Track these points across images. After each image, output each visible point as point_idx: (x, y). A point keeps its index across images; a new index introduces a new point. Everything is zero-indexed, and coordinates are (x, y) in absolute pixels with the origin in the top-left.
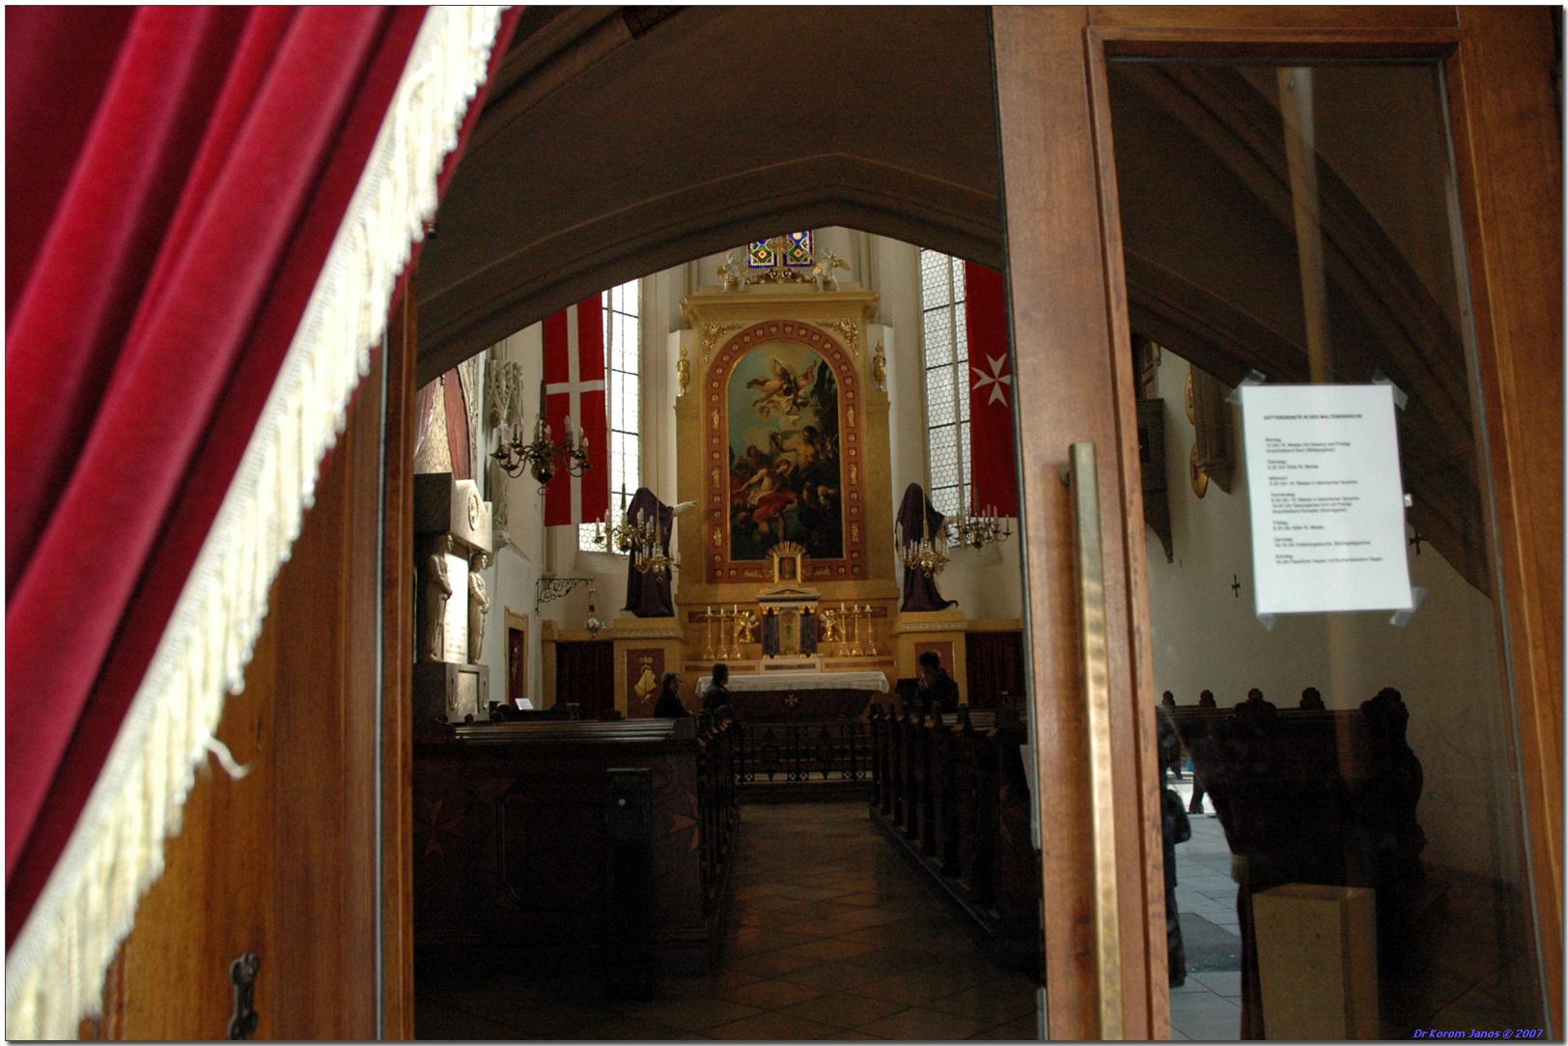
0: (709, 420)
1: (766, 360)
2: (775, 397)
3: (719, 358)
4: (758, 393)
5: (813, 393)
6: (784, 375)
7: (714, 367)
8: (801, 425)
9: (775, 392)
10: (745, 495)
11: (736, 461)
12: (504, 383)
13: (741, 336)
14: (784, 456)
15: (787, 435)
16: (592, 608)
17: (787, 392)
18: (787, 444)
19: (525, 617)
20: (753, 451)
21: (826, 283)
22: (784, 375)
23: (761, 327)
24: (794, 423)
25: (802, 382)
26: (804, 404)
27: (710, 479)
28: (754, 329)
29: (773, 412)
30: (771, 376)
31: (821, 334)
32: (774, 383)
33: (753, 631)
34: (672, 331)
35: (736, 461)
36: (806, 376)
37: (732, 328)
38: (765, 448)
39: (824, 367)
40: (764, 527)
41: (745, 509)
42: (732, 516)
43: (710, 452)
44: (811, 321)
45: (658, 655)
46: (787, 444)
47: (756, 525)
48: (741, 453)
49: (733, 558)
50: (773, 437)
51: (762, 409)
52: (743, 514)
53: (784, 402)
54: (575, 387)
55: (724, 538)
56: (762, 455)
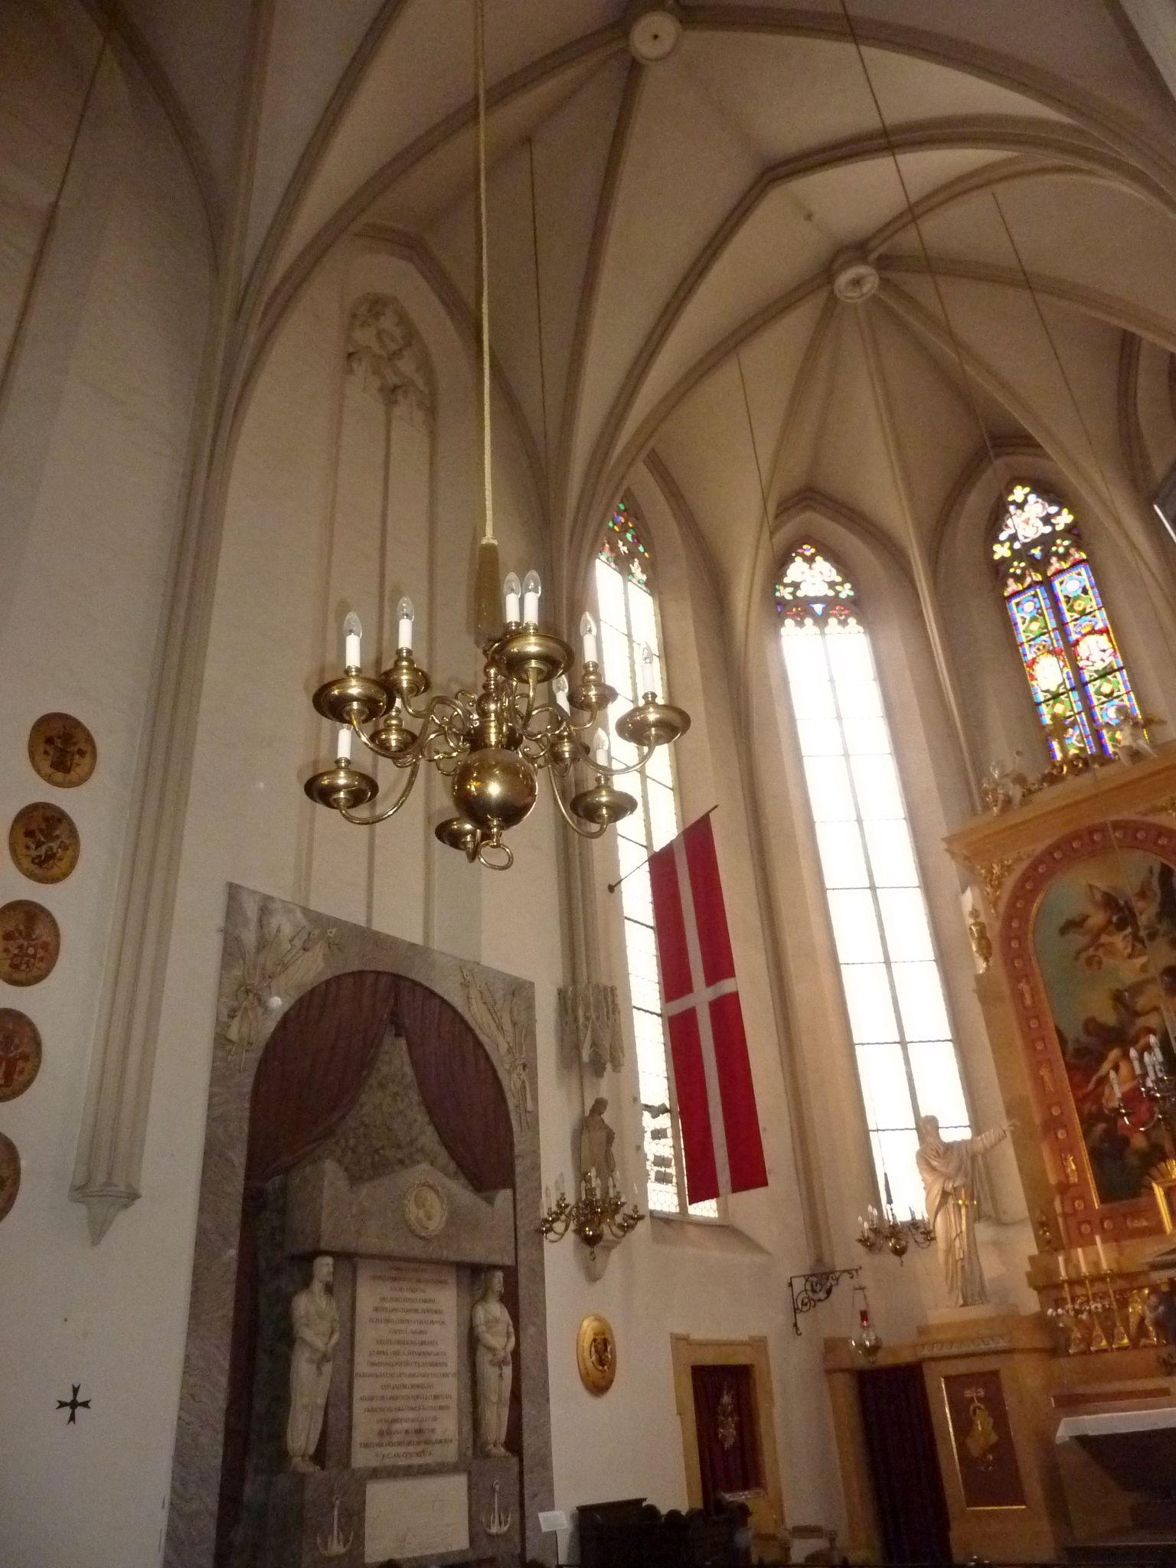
0: (1019, 996)
1: (1075, 891)
2: (1105, 939)
3: (1012, 904)
4: (1079, 939)
5: (1160, 916)
6: (1110, 902)
7: (1008, 920)
8: (1153, 972)
9: (1104, 929)
10: (1097, 1096)
11: (1071, 1047)
12: (581, 1013)
13: (1033, 867)
14: (1141, 1022)
15: (1137, 989)
16: (864, 1316)
17: (1120, 926)
18: (1142, 1002)
19: (759, 1344)
20: (1092, 1026)
21: (1135, 755)
22: (1110, 902)
23: (1057, 846)
24: (1144, 968)
25: (1138, 905)
26: (1152, 936)
27: (1039, 1082)
28: (1049, 852)
29: (1108, 962)
30: (1090, 909)
31: (1149, 827)
32: (1098, 918)
33: (1157, 1324)
34: (963, 891)
35: (1071, 1047)
36: (1142, 895)
37: (1019, 860)
38: (1109, 1017)
39: (1166, 872)
40: (1139, 1141)
41: (1107, 1119)
42: (1086, 1134)
43: (1030, 1046)
44: (1129, 815)
45: (990, 1380)
46: (1142, 1002)
47: (1126, 1141)
48: (1074, 1031)
49: (1103, 1200)
50: (1117, 997)
51: (1089, 961)
52: (1101, 1127)
53: (1119, 941)
54: (701, 996)
55: (1080, 1170)
56: (1113, 1028)
